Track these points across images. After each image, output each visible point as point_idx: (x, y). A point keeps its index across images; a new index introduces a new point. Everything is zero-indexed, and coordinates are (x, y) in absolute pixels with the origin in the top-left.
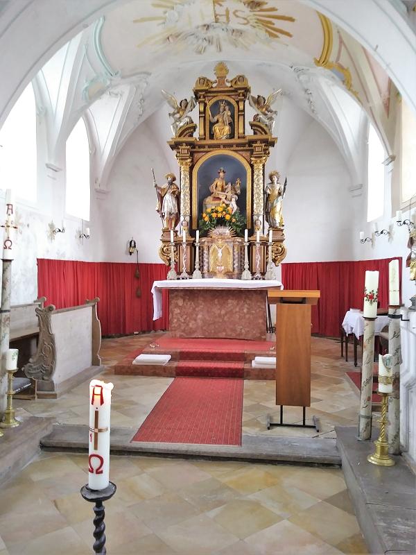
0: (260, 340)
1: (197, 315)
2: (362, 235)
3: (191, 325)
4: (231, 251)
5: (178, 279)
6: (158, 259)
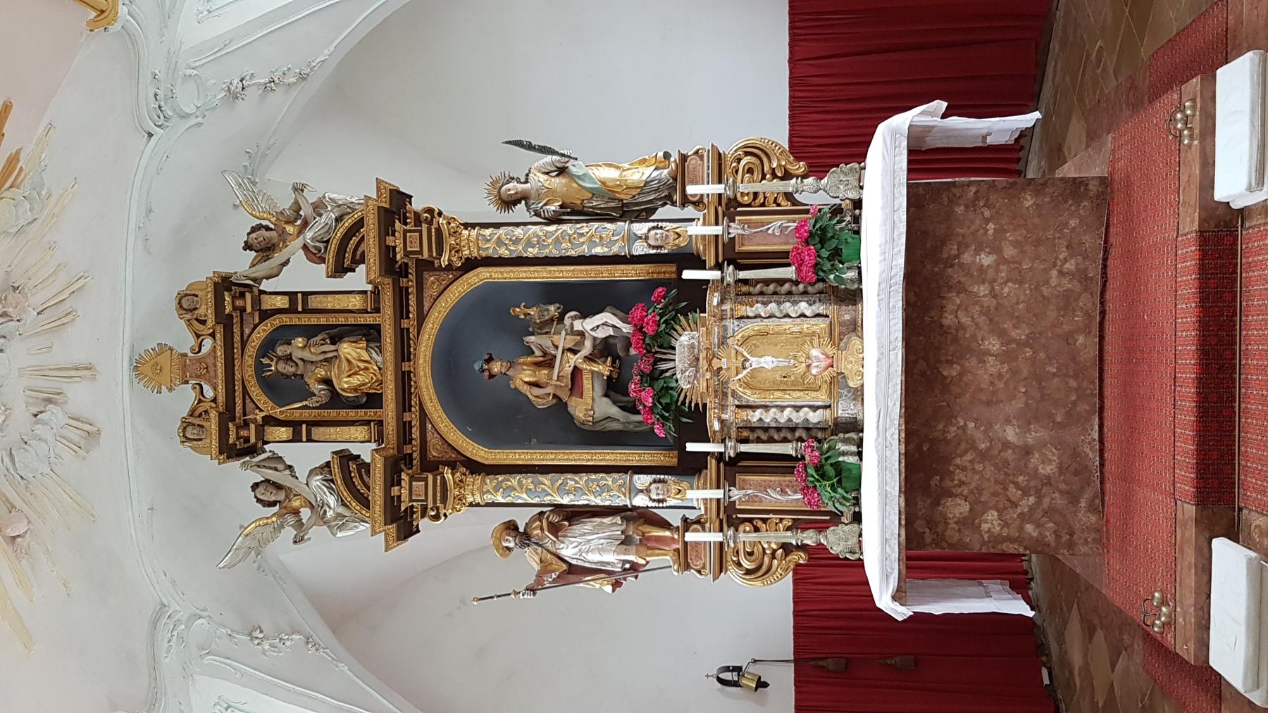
1: (1006, 445)
3: (1048, 470)
4: (756, 326)
5: (857, 518)
6: (778, 594)
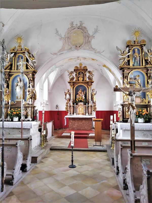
0: (91, 130)
2: (114, 105)
3: (74, 127)
6: (64, 110)
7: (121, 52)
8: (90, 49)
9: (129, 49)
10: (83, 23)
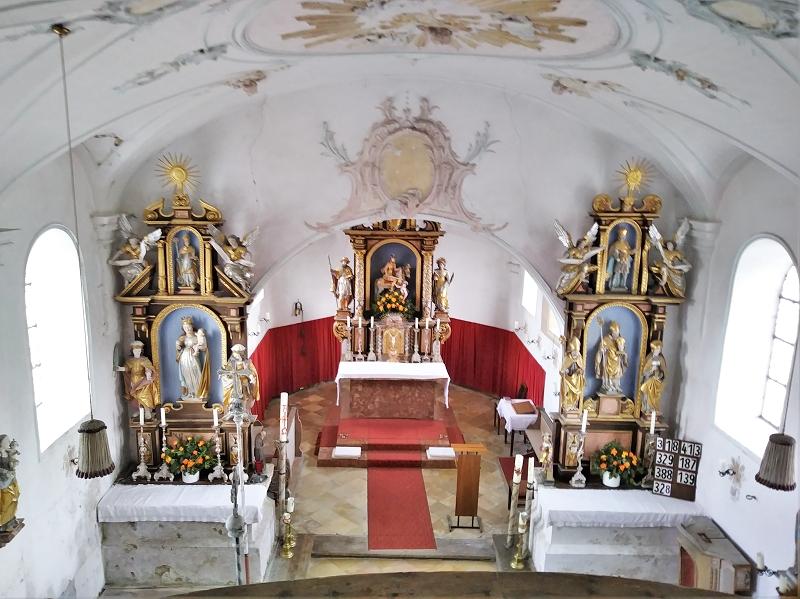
7: (570, 239)
8: (455, 213)
9: (599, 229)
10: (434, 107)
